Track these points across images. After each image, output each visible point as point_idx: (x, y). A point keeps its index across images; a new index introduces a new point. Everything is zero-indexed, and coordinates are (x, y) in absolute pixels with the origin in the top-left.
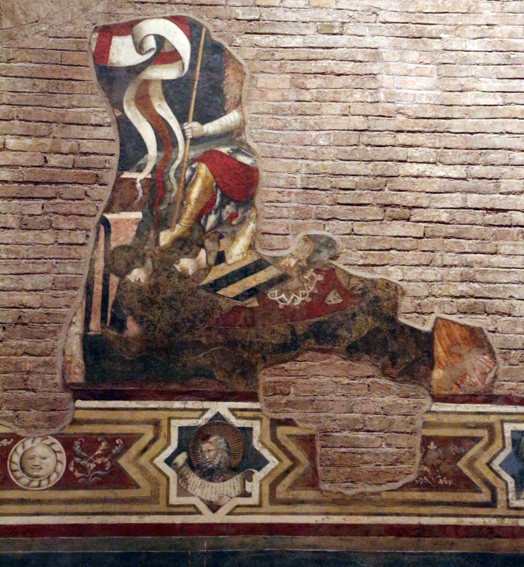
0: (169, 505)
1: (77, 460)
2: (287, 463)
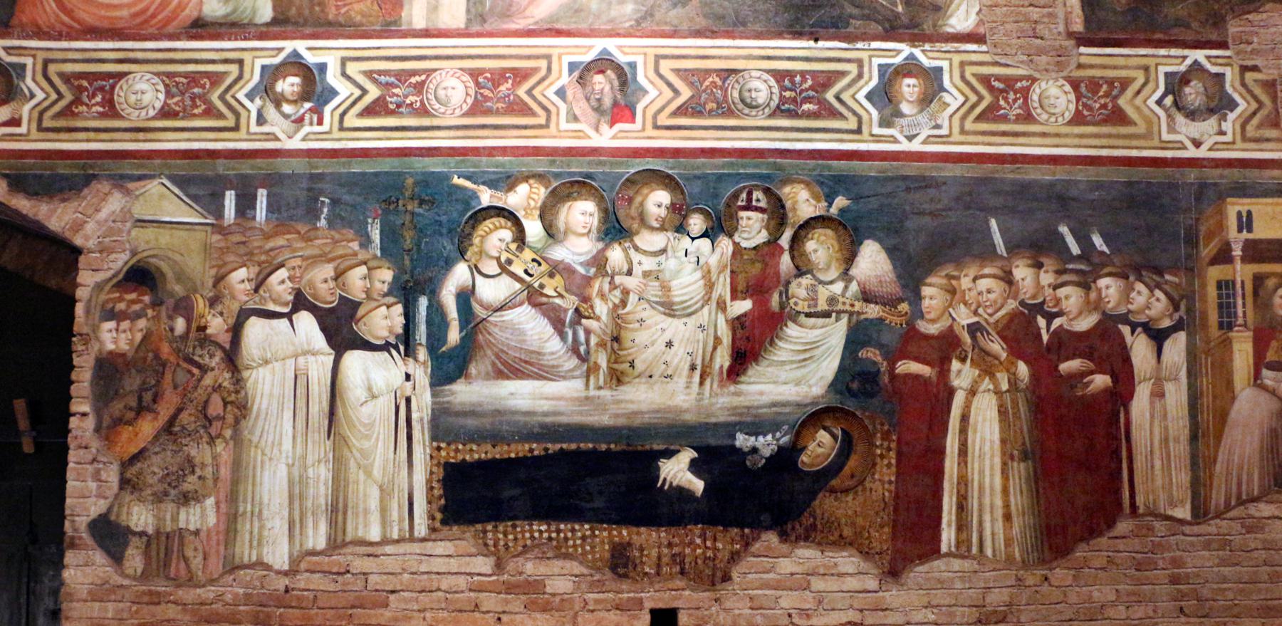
0: (1162, 141)
1: (1084, 100)
2: (1254, 105)
